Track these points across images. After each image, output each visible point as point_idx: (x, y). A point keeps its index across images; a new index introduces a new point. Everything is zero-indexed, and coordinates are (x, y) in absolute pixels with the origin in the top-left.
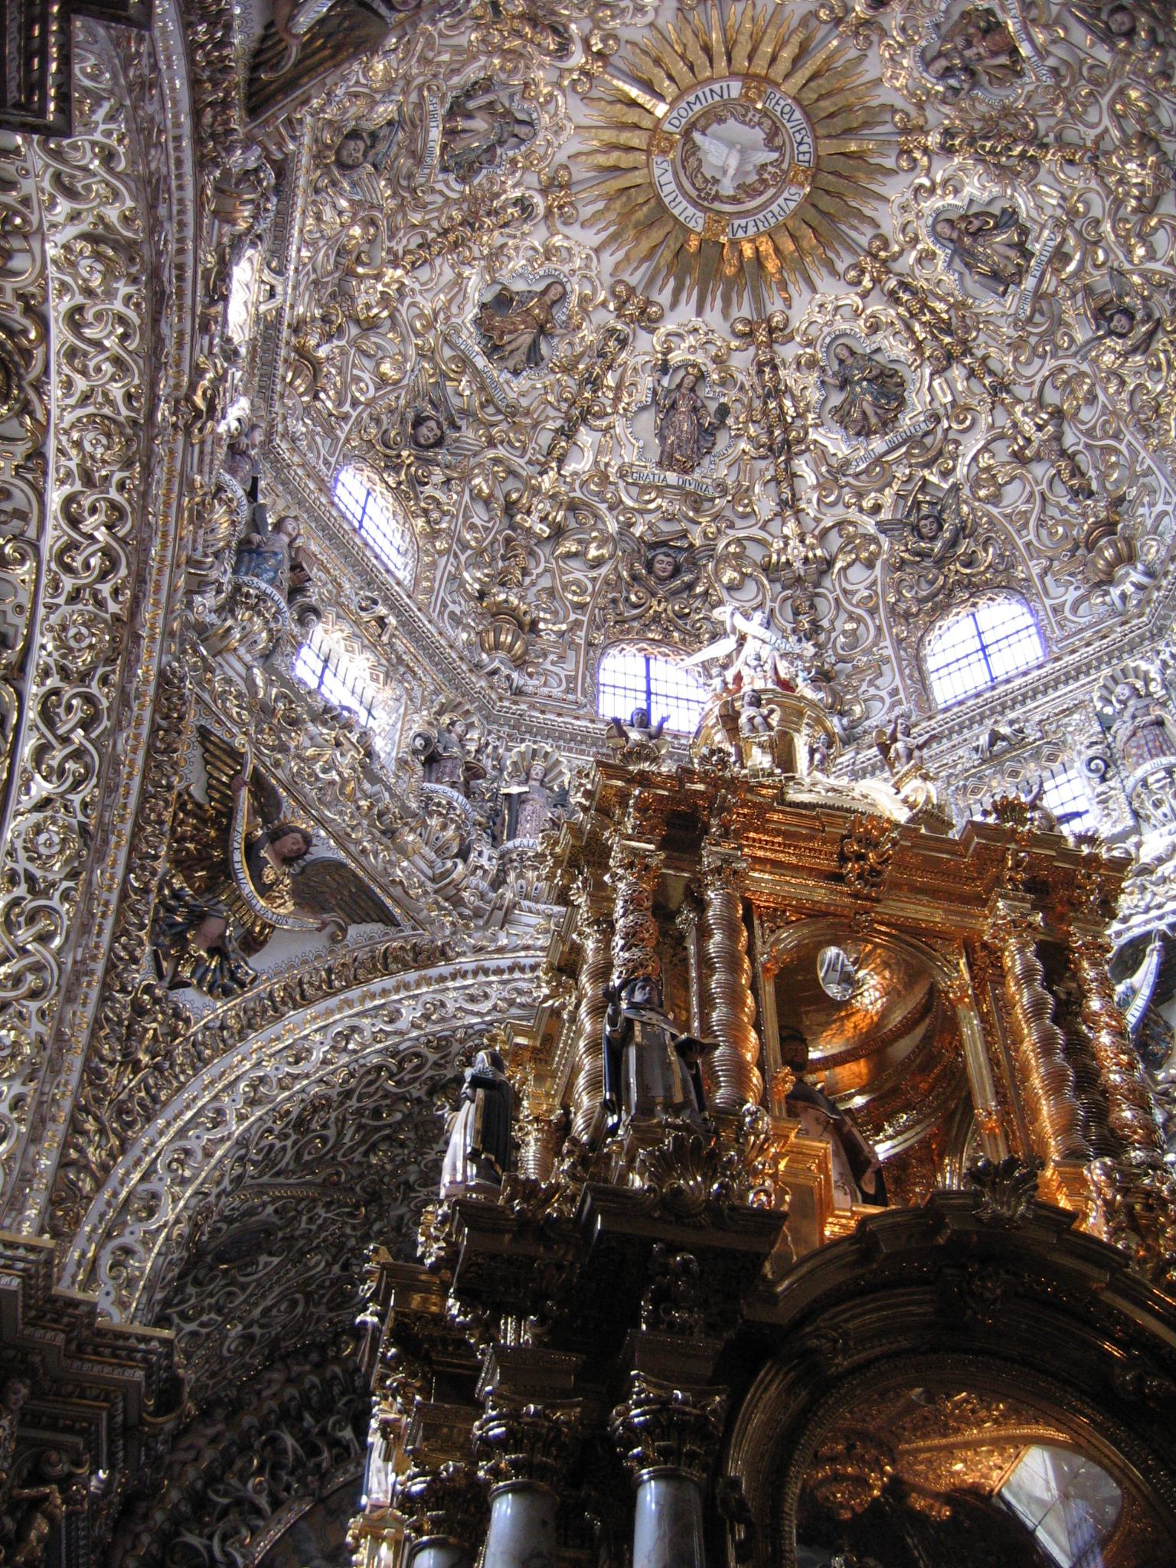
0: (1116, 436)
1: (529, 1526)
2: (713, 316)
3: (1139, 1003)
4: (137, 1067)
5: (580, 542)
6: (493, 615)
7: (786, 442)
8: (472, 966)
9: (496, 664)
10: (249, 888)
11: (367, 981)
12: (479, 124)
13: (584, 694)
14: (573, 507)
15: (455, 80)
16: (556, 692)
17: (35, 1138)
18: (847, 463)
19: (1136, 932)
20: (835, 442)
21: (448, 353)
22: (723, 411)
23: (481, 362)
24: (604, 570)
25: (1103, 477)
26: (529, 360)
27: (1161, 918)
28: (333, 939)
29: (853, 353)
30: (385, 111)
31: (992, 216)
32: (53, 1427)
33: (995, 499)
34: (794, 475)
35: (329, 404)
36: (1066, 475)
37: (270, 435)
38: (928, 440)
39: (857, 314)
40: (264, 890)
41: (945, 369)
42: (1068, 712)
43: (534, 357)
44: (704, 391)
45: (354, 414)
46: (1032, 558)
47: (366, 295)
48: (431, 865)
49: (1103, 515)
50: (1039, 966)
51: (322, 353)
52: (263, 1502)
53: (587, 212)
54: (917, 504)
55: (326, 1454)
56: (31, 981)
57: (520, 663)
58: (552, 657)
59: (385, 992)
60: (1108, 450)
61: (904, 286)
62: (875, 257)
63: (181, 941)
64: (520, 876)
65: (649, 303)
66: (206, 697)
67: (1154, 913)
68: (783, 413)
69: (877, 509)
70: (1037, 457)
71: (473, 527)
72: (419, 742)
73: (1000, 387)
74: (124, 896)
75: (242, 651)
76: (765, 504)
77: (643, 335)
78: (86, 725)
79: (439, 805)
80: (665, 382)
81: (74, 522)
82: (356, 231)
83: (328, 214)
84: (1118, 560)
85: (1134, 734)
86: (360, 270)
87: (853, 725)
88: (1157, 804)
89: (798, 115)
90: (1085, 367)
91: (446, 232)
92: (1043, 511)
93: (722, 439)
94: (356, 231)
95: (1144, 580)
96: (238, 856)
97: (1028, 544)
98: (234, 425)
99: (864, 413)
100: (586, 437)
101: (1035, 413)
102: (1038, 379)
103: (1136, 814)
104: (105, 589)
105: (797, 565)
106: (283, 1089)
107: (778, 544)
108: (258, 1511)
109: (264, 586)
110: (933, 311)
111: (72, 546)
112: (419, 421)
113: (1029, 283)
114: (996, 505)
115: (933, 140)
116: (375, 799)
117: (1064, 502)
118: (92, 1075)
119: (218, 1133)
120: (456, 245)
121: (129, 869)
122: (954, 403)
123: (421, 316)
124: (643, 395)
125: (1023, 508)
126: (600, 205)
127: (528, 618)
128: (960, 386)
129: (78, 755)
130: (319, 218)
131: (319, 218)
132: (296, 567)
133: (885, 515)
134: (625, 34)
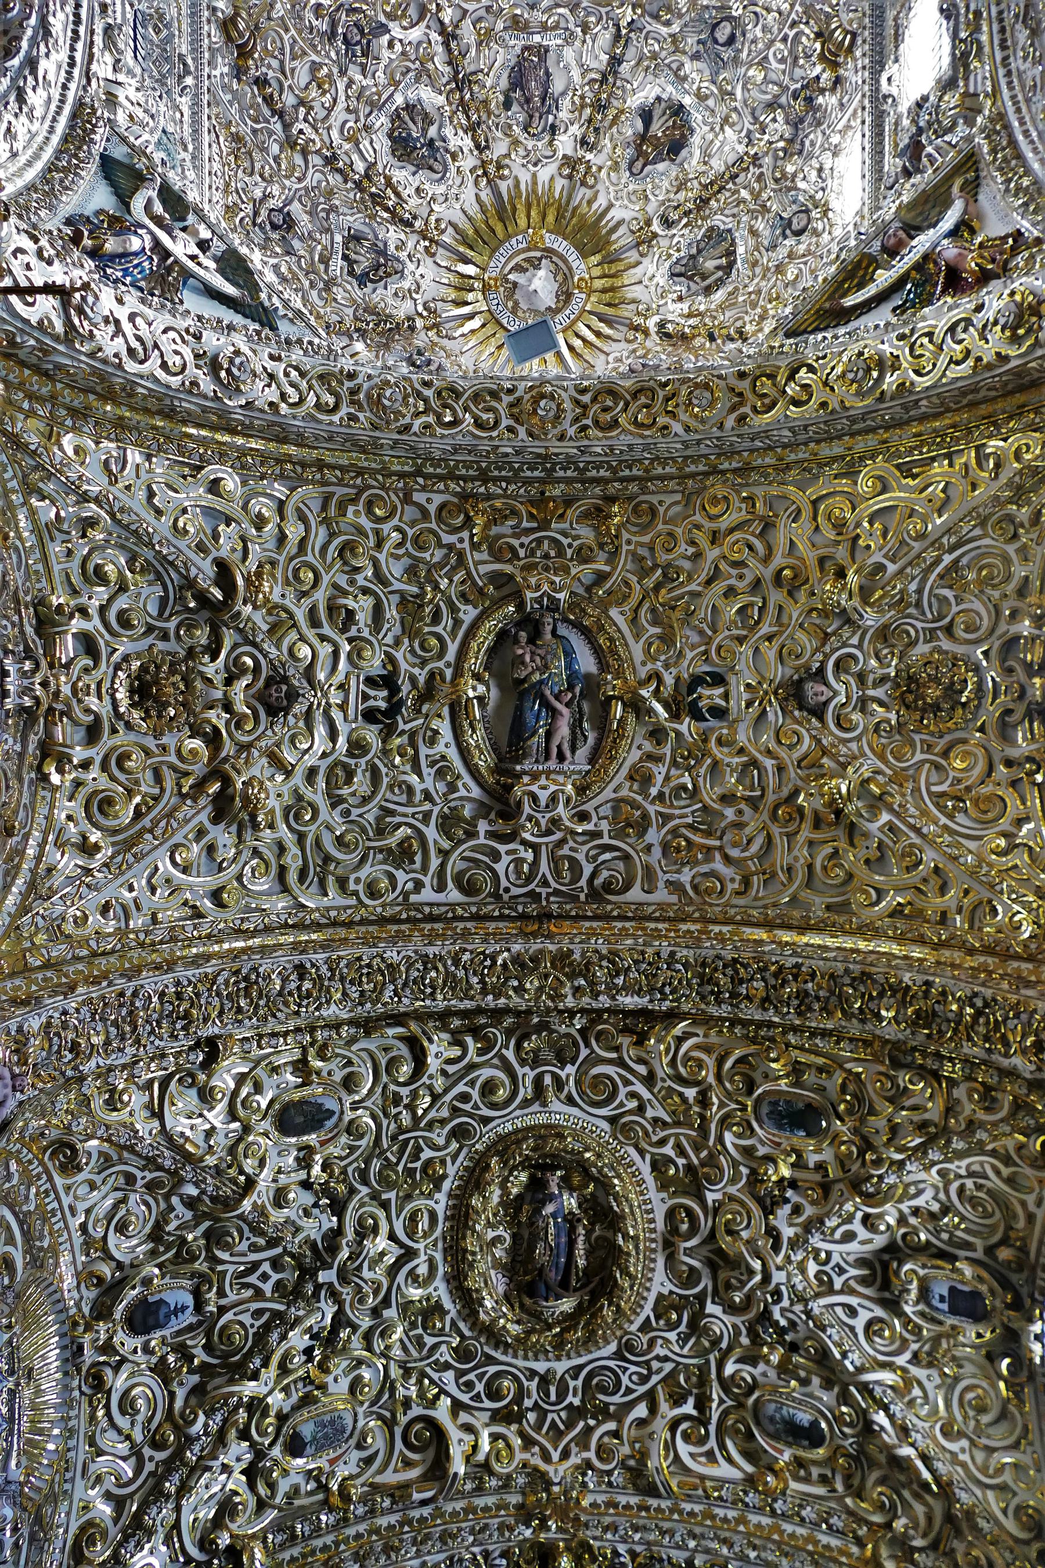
0: (255, 131)
2: (524, 177)
12: (710, 265)
15: (730, 288)
18: (417, 80)
22: (507, 105)
23: (687, 101)
25: (254, 96)
26: (650, 111)
29: (431, 168)
30: (782, 252)
31: (372, 281)
33: (315, 67)
34: (450, 63)
35: (807, 31)
38: (368, 109)
39: (433, 199)
44: (521, 117)
46: (282, 18)
47: (779, 126)
51: (818, 69)
53: (622, 230)
54: (365, 54)
60: (257, 121)
61: (408, 224)
62: (431, 241)
65: (570, 177)
68: (466, 113)
69: (391, 45)
70: (296, 107)
73: (330, 161)
76: (468, 33)
77: (569, 152)
82: (790, 169)
83: (813, 175)
86: (781, 144)
89: (505, 322)
90: (287, 183)
91: (722, 188)
92: (282, 62)
93: (504, 83)
94: (790, 169)
97: (287, 30)
102: (311, 171)
110: (387, 209)
112: (731, 40)
113: (338, 238)
115: (419, 323)
117: (271, 74)
120: (712, 183)
122: (357, 144)
123: (732, 125)
124: (566, 103)
125: (296, 63)
126: (614, 237)
128: (355, 157)
130: (820, 170)
131: (820, 170)
133: (385, 39)
134: (623, 345)
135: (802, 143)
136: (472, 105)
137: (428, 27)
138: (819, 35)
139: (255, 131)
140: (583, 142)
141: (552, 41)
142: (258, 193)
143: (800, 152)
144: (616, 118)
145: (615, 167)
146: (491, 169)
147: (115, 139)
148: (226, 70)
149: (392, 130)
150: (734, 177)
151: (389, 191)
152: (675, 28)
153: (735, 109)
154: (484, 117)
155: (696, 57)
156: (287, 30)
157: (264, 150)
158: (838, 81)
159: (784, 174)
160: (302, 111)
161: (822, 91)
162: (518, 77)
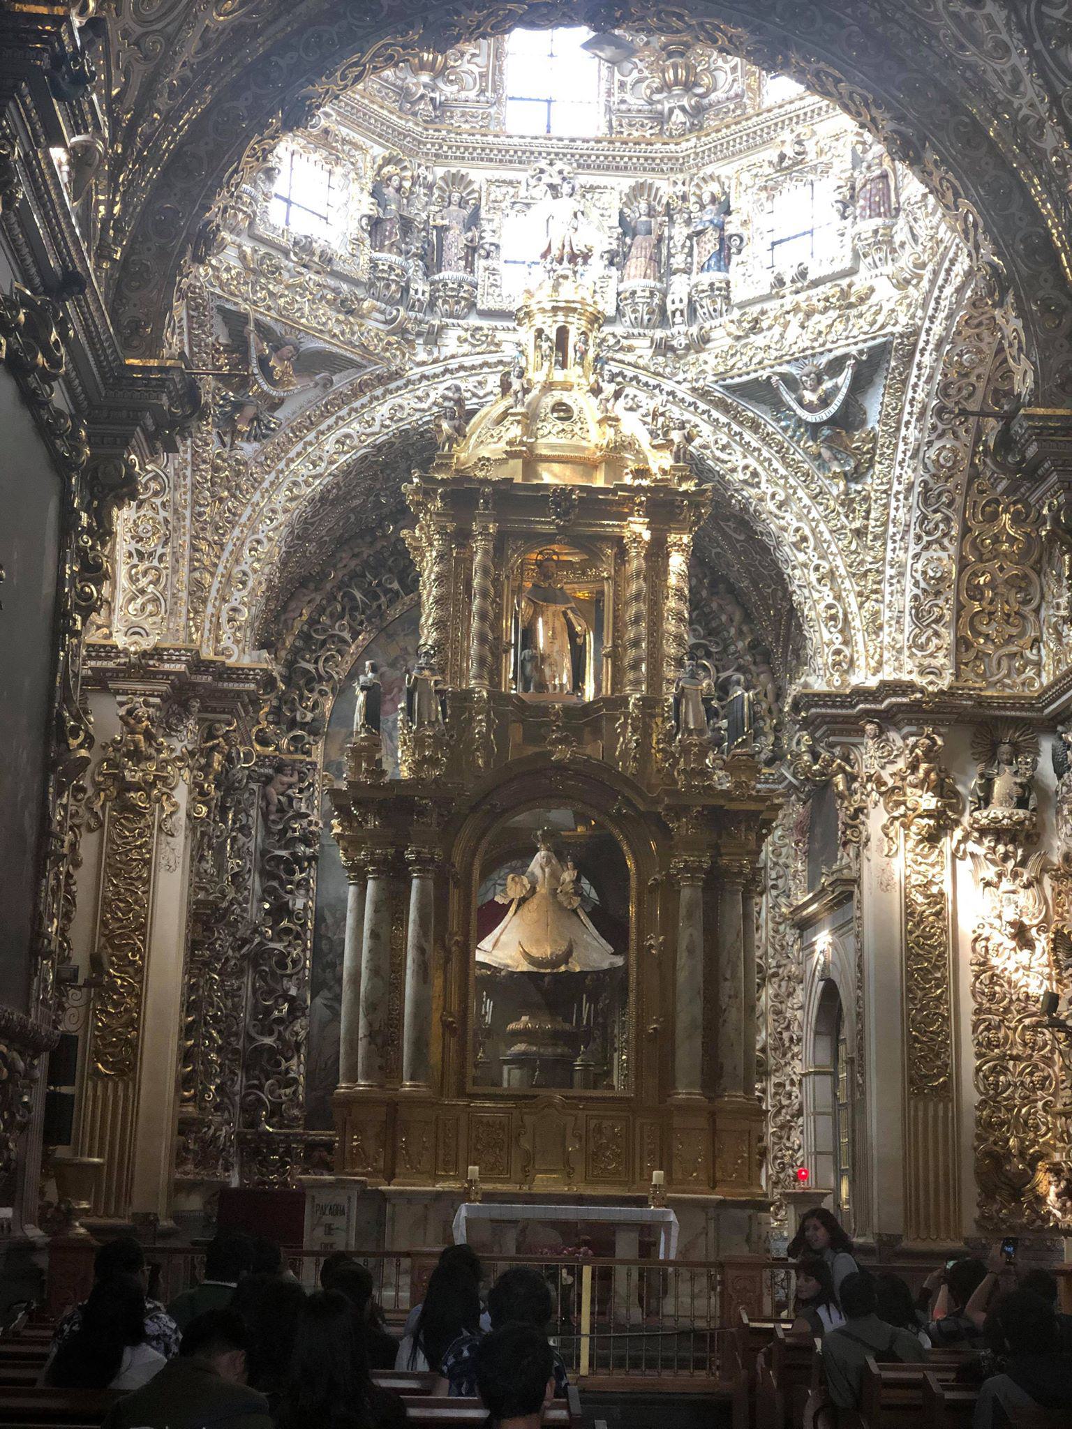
1: (379, 890)
3: (841, 397)
4: (221, 500)
8: (418, 376)
9: (421, 91)
10: (265, 387)
11: (350, 402)
13: (494, 91)
27: (856, 344)
28: (325, 386)
48: (382, 312)
52: (347, 635)
55: (383, 599)
58: (467, 57)
59: (363, 406)
64: (445, 302)
66: (218, 291)
67: (851, 341)
72: (364, 221)
79: (383, 271)
85: (865, 186)
103: (856, 256)
106: (310, 486)
108: (344, 641)
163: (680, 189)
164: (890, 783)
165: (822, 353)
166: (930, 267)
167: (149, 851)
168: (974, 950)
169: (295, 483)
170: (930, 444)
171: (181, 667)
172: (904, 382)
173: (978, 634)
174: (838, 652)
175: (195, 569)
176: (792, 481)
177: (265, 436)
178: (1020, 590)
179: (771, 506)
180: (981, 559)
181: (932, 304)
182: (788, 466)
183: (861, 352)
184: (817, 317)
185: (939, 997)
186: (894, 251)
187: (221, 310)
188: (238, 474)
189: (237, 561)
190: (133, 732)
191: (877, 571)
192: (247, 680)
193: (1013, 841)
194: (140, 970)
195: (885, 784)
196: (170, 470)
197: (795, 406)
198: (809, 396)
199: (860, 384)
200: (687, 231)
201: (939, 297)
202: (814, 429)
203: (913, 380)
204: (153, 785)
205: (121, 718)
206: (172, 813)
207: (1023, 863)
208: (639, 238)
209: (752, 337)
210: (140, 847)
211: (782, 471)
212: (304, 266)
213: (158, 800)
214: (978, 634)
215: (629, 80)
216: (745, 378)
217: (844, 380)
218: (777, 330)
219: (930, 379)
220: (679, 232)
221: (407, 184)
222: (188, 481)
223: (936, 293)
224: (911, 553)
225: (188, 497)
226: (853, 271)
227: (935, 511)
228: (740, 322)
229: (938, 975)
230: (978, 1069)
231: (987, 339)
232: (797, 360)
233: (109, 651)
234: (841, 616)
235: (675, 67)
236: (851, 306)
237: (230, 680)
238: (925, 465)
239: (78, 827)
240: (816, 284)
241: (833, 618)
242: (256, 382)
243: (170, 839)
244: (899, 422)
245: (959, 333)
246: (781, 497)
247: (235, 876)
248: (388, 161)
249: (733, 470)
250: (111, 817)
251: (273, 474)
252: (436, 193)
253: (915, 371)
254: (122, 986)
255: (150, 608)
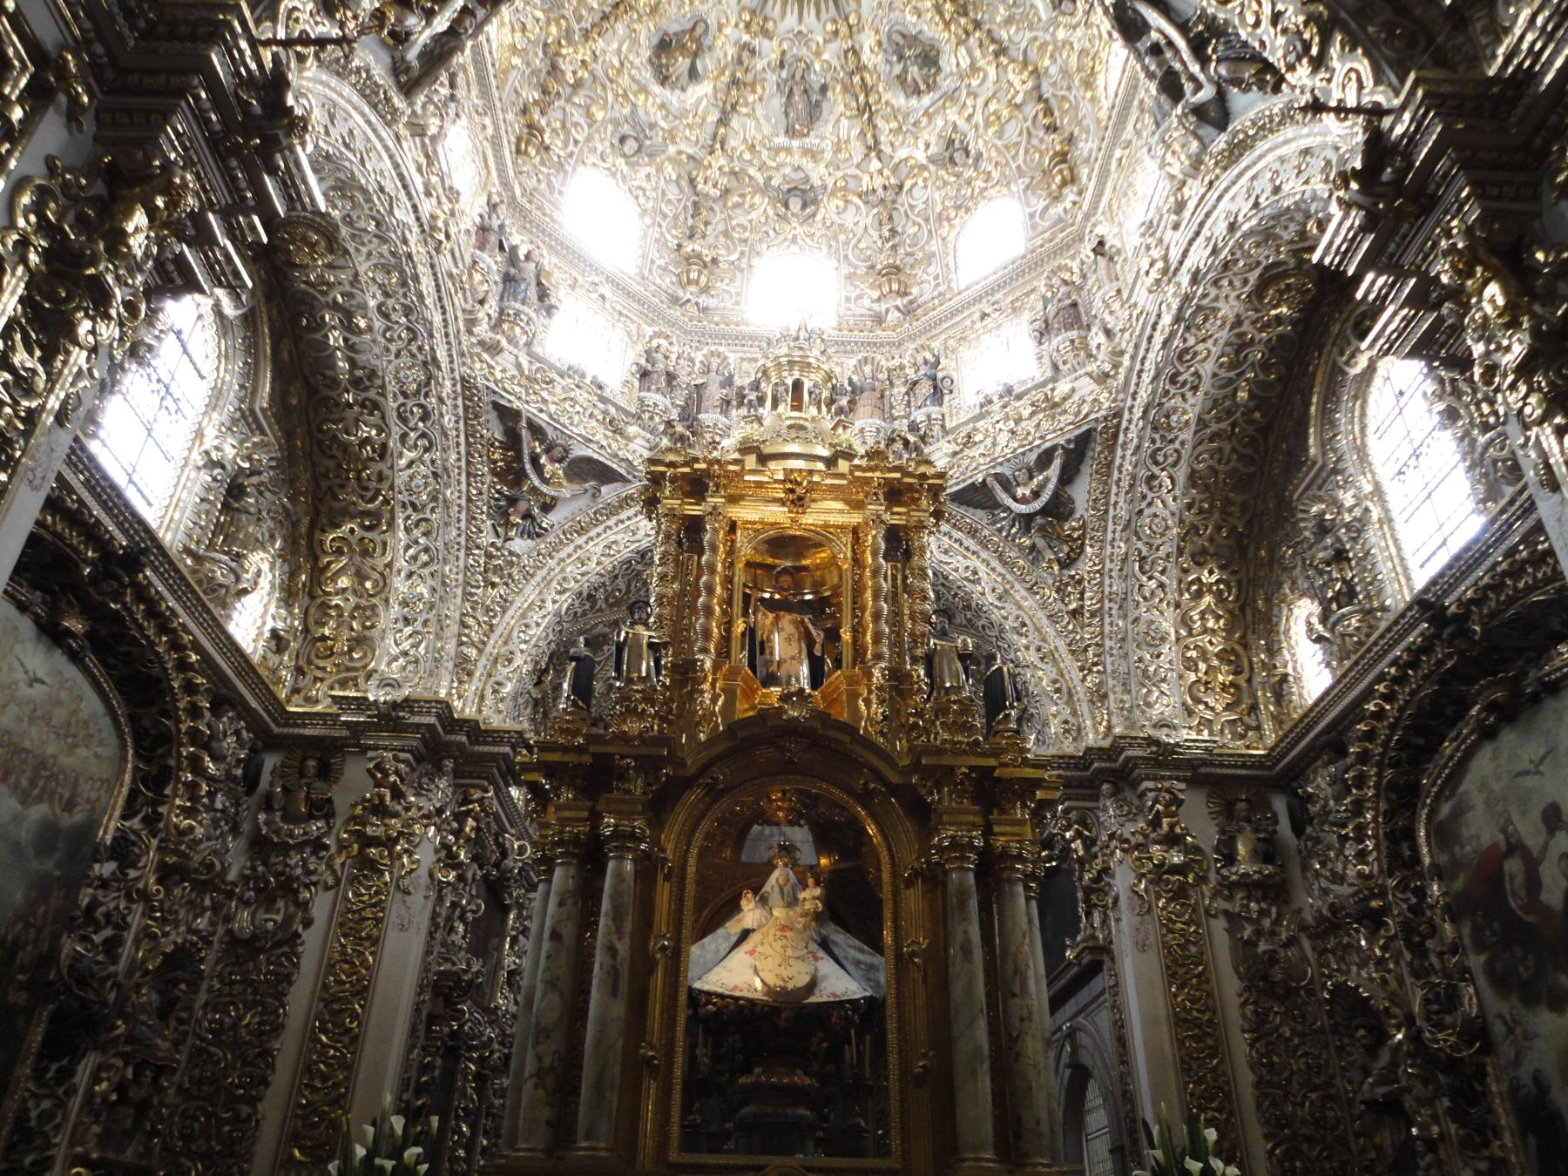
3: (1051, 486)
4: (493, 585)
5: (742, 196)
6: (687, 260)
7: (867, 103)
9: (688, 296)
10: (537, 482)
14: (733, 173)
16: (729, 305)
17: (438, 637)
19: (1048, 445)
20: (899, 100)
21: (635, 87)
22: (824, 89)
23: (656, 88)
24: (754, 215)
28: (594, 496)
29: (904, 36)
32: (471, 777)
33: (1000, 134)
34: (875, 127)
36: (1041, 116)
37: (514, 198)
40: (545, 481)
41: (964, 42)
42: (1027, 294)
43: (693, 74)
45: (576, 151)
49: (1058, 148)
50: (883, 546)
54: (951, 142)
56: (425, 558)
57: (706, 290)
60: (1064, 98)
63: (506, 515)
65: (766, 19)
66: (492, 385)
71: (669, 201)
72: (634, 368)
73: (1001, 51)
74: (469, 500)
75: (511, 348)
77: (766, 42)
78: (422, 419)
80: (784, 74)
81: (386, 316)
84: (1064, 183)
87: (911, 302)
88: (1065, 363)
90: (1048, 38)
92: (1029, 142)
93: (825, 105)
94: (554, 30)
95: (1076, 198)
96: (528, 466)
97: (1018, 167)
98: (478, 220)
99: (914, 80)
100: (735, 122)
101: (1021, 73)
103: (1056, 367)
104: (414, 348)
105: (880, 191)
107: (866, 178)
109: (518, 306)
111: (388, 329)
112: (623, 140)
114: (1000, 138)
116: (605, 413)
117: (1041, 133)
118: (467, 595)
119: (543, 612)
121: (469, 485)
123: (613, 66)
125: (1015, 139)
127: (708, 259)
129: (423, 435)
130: (524, 29)
131: (524, 29)
132: (539, 284)
133: (933, 150)
135: (545, 53)
136: (858, 90)
137: (892, 157)
138: (547, 149)
139: (1069, 88)
140: (753, 52)
141: (781, 140)
142: (1079, 32)
143: (546, 45)
144: (722, 73)
145: (720, 28)
146: (844, 30)
147: (1206, 140)
148: (1081, 145)
149: (937, 73)
150: (605, 17)
151: (947, 17)
152: (672, 150)
153: (611, 81)
154: (847, 80)
155: (652, 126)
156: (1018, 167)
157: (1065, 72)
158: (525, 111)
159: (558, 24)
160: (1018, 100)
161: (536, 102)
162: (814, 113)
163: (896, 362)
164: (1133, 842)
165: (1031, 450)
166: (1127, 357)
167: (382, 910)
168: (1244, 1016)
169: (564, 579)
170: (1141, 512)
171: (432, 720)
172: (1109, 465)
173: (1198, 701)
174: (1066, 722)
175: (461, 644)
176: (1009, 577)
177: (539, 535)
178: (1230, 662)
179: (990, 598)
180: (1190, 634)
181: (1134, 380)
182: (1004, 563)
183: (1069, 441)
184: (1024, 424)
185: (1215, 1069)
186: (1090, 355)
187: (496, 406)
188: (511, 564)
189: (506, 643)
190: (378, 784)
191: (1097, 644)
192: (501, 743)
193: (1265, 898)
194: (354, 1039)
195: (1127, 841)
196: (440, 544)
197: (1009, 502)
198: (1020, 492)
199: (1067, 477)
200: (903, 390)
201: (1141, 371)
202: (1027, 521)
203: (1118, 461)
204: (396, 841)
205: (369, 770)
206: (412, 871)
207: (1277, 922)
208: (865, 394)
209: (966, 452)
210: (374, 905)
211: (1000, 569)
212: (578, 387)
213: (400, 857)
214: (1198, 701)
215: (853, 296)
216: (962, 485)
217: (1054, 471)
218: (988, 442)
219: (1138, 448)
220: (900, 390)
221: (674, 357)
222: (461, 563)
223: (1138, 366)
224: (1130, 619)
225: (461, 577)
226: (1054, 379)
227: (1150, 578)
228: (955, 440)
229: (1210, 1042)
230: (1271, 1153)
231: (1191, 400)
232: (1008, 460)
233: (362, 704)
234: (1065, 689)
235: (890, 282)
236: (1056, 405)
237: (486, 743)
238: (1136, 533)
239: (315, 884)
240: (1019, 397)
241: (1058, 691)
242: (527, 477)
243: (408, 898)
244: (1107, 504)
245: (1167, 393)
246: (1000, 590)
247: (511, 973)
248: (657, 335)
249: (956, 570)
250: (350, 874)
251: (545, 571)
252: (698, 365)
253: (1119, 452)
254: (334, 1057)
255: (410, 667)
